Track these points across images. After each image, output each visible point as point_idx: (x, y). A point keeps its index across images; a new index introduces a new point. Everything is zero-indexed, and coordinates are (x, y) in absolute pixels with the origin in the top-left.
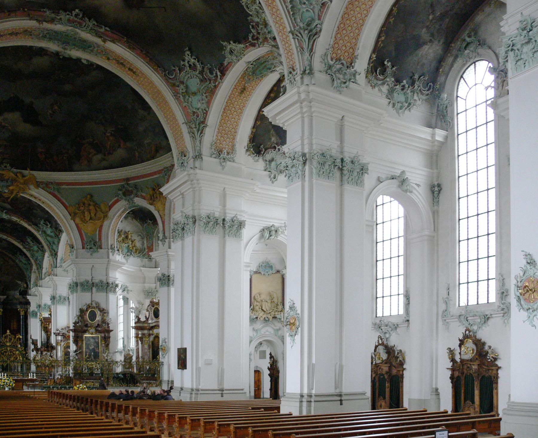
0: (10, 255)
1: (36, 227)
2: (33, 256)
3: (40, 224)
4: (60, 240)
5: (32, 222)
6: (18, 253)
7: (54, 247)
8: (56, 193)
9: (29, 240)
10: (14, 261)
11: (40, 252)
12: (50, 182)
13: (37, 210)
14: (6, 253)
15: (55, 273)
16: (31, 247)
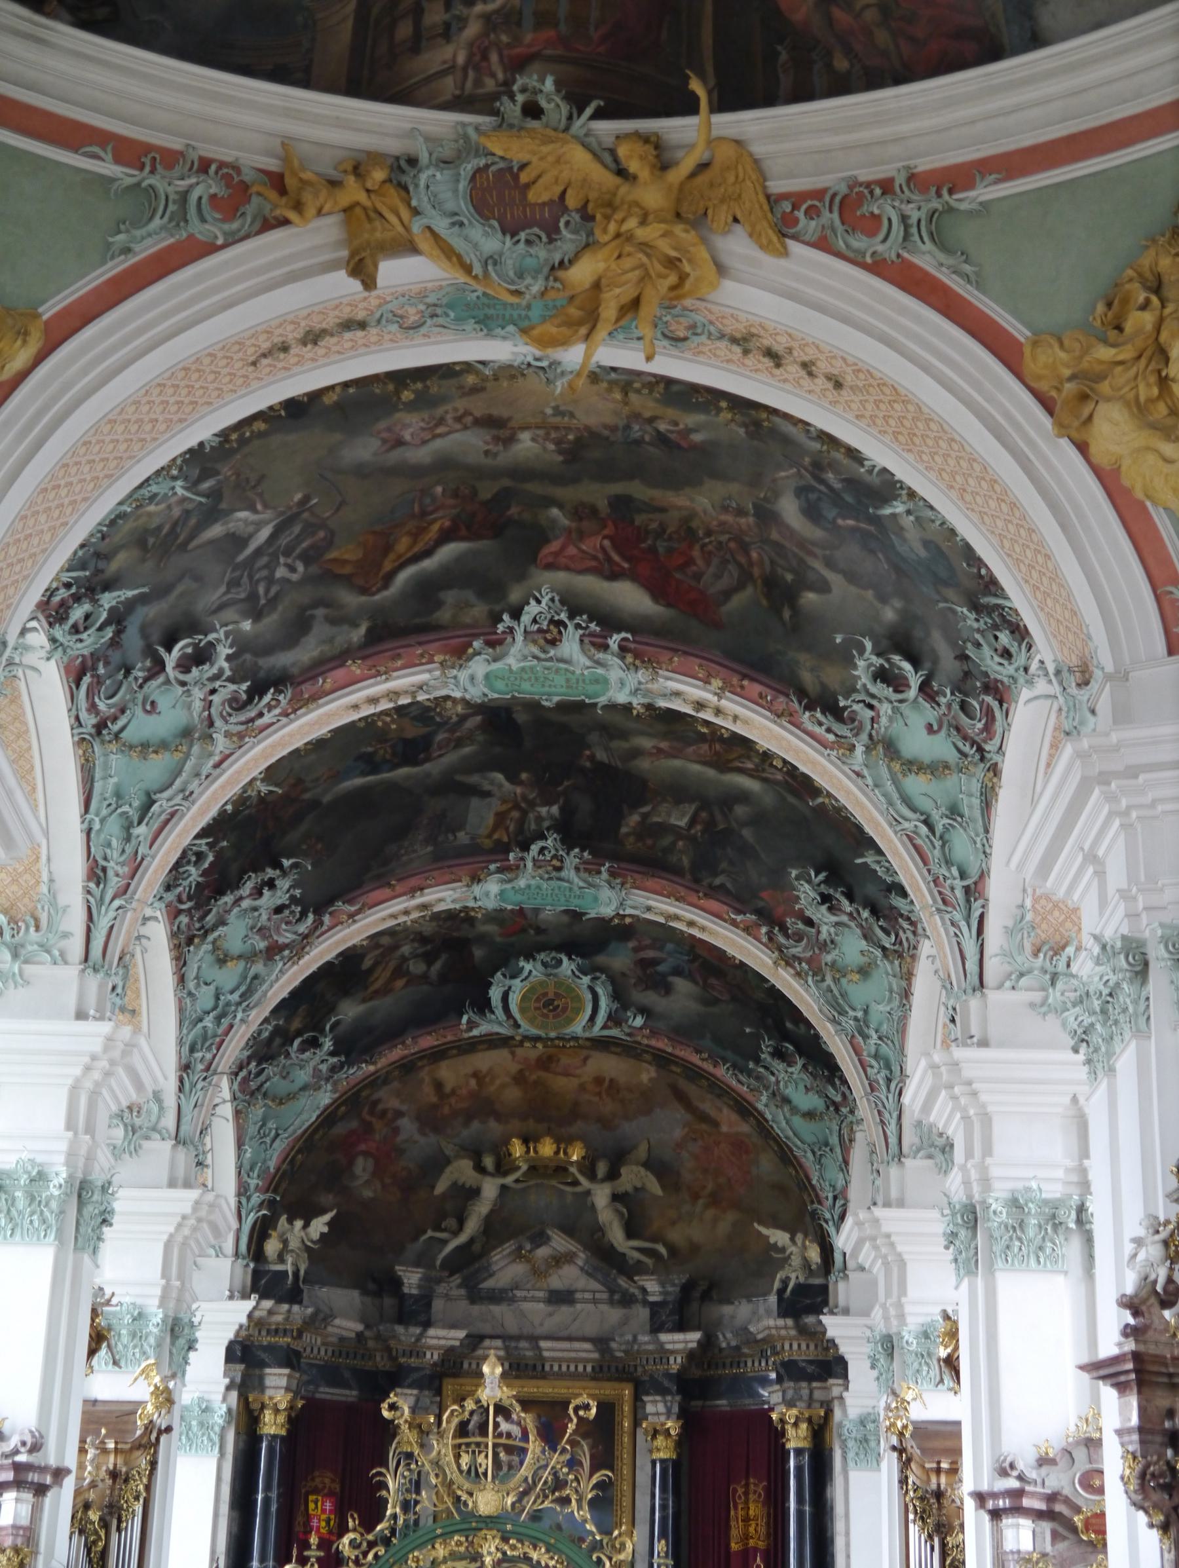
0: (722, 1072)
1: (828, 721)
2: (837, 1006)
3: (850, 690)
4: (995, 770)
5: (801, 693)
6: (767, 1046)
7: (962, 846)
8: (927, 258)
9: (806, 894)
10: (745, 1110)
11: (885, 966)
12: (868, 185)
13: (823, 587)
14: (695, 1059)
15: (974, 1030)
16: (824, 947)
